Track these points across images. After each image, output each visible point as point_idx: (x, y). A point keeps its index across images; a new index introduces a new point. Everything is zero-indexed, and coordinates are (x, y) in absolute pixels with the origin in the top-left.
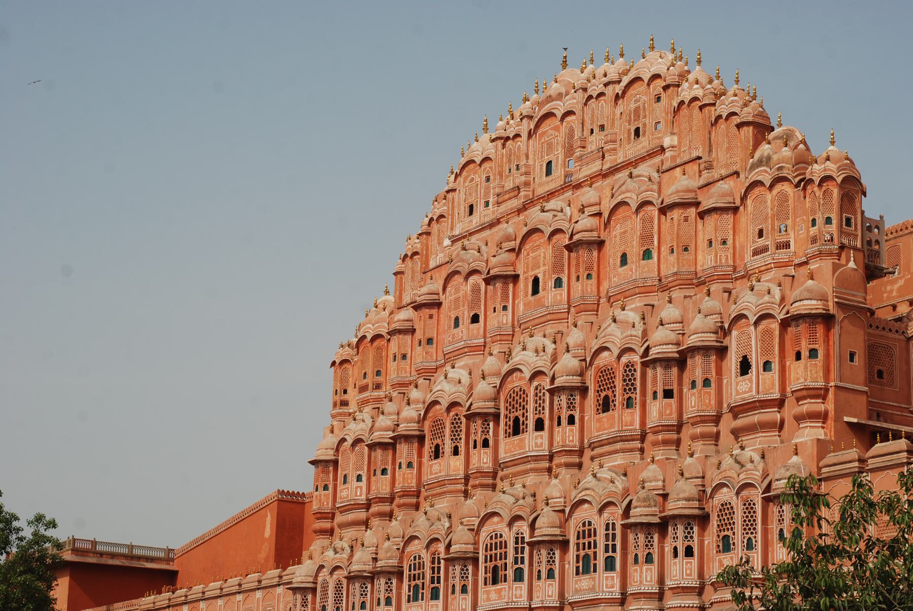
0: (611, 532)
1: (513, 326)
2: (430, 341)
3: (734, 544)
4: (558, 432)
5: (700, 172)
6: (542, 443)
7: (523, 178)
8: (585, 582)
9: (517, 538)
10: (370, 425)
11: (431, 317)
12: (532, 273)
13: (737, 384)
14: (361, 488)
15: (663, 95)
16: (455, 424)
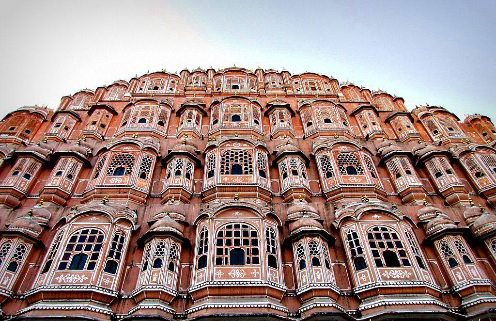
2: (103, 126)
4: (297, 178)
9: (267, 232)
16: (146, 163)
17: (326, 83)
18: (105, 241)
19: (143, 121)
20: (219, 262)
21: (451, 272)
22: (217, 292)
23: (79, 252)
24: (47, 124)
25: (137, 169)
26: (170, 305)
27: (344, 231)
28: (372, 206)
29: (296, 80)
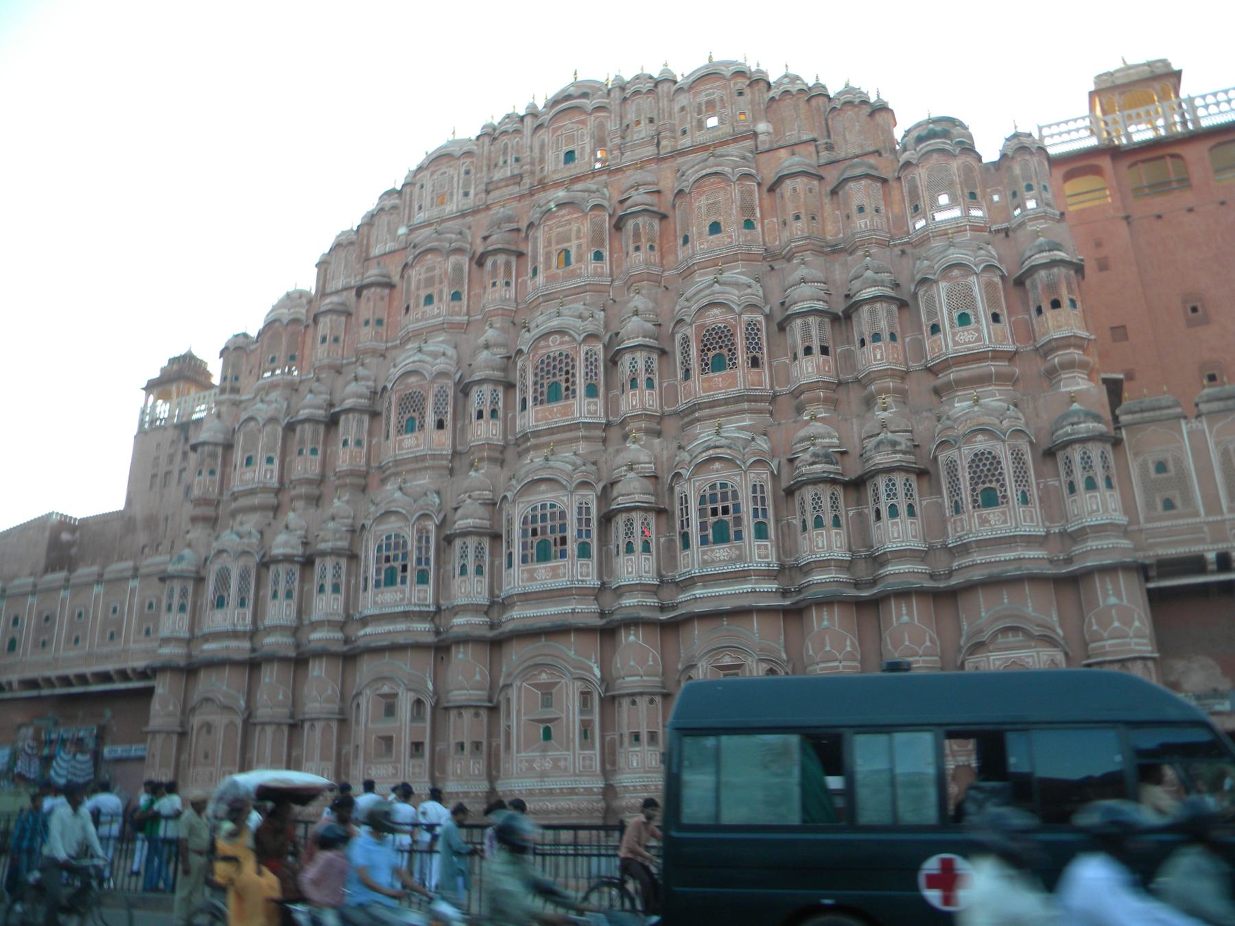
0: (759, 494)
1: (516, 301)
2: (380, 322)
3: (1004, 497)
4: (634, 395)
5: (818, 152)
6: (596, 411)
7: (527, 167)
8: (721, 552)
9: (580, 508)
10: (285, 406)
11: (382, 298)
12: (555, 248)
13: (954, 335)
14: (272, 471)
15: (747, 91)
17: (741, 94)
18: (409, 547)
19: (429, 299)
20: (524, 560)
21: (800, 537)
22: (523, 598)
23: (388, 565)
24: (310, 331)
25: (430, 419)
26: (486, 613)
27: (677, 489)
28: (716, 447)
29: (683, 100)
